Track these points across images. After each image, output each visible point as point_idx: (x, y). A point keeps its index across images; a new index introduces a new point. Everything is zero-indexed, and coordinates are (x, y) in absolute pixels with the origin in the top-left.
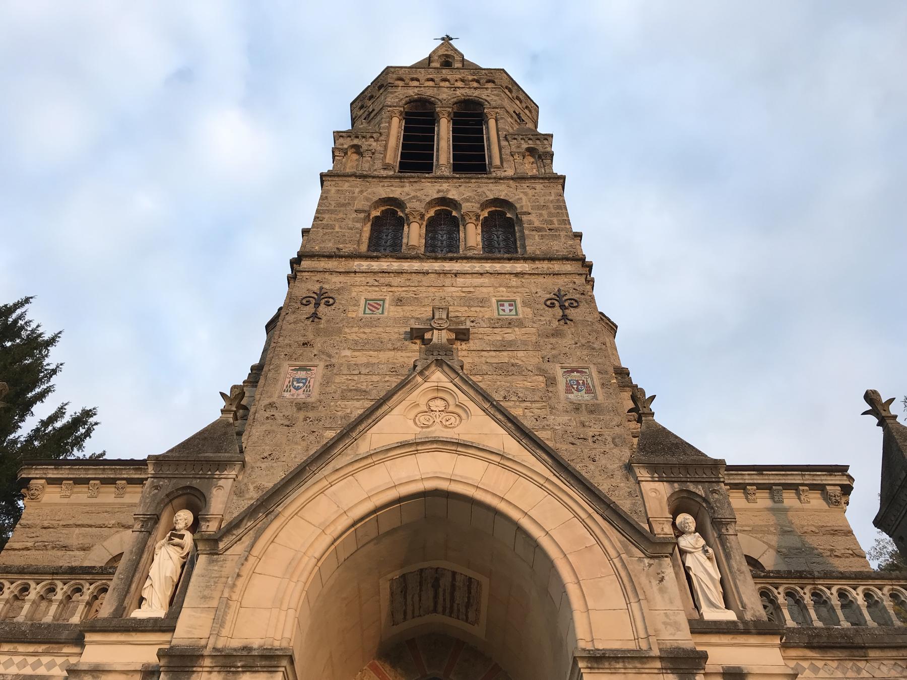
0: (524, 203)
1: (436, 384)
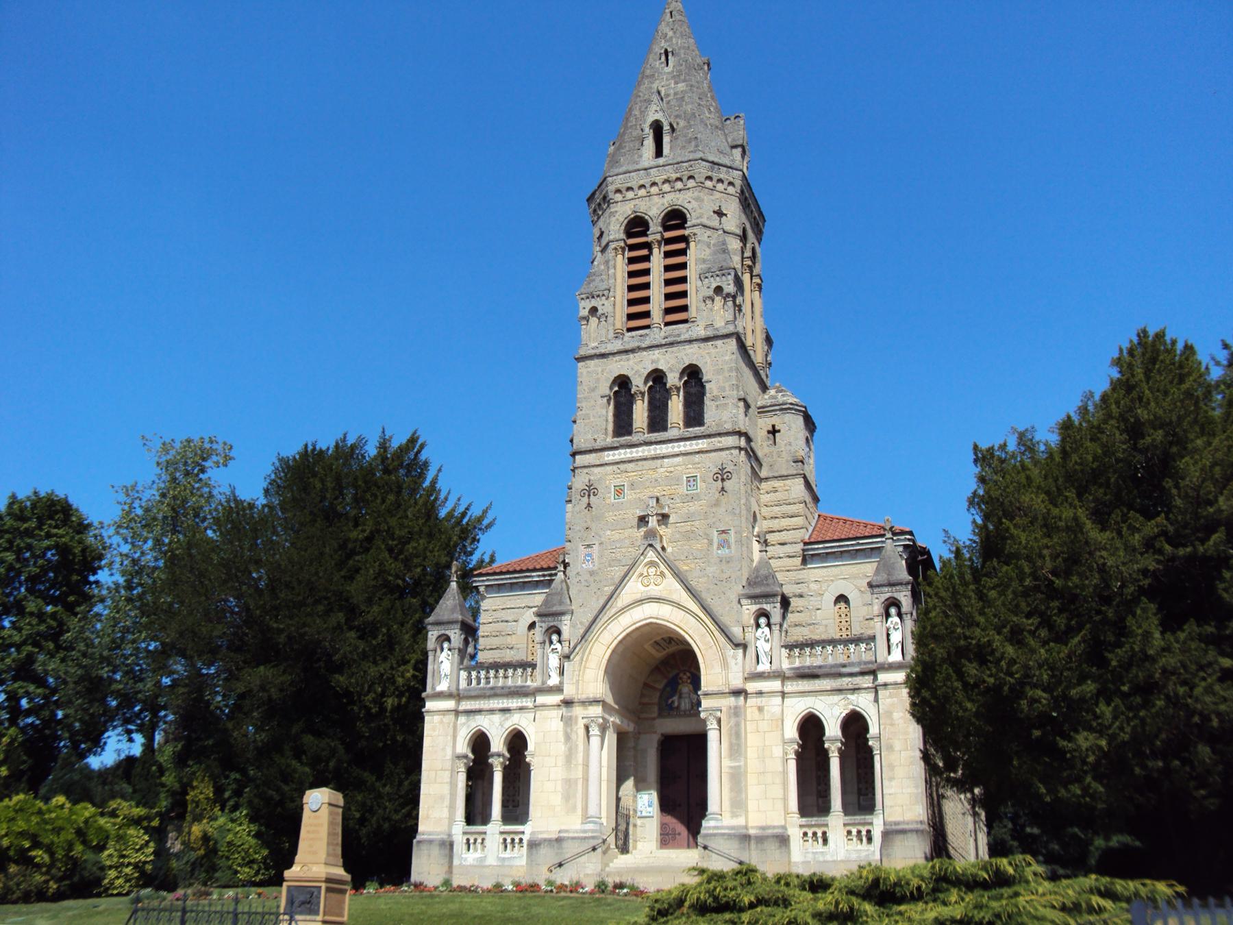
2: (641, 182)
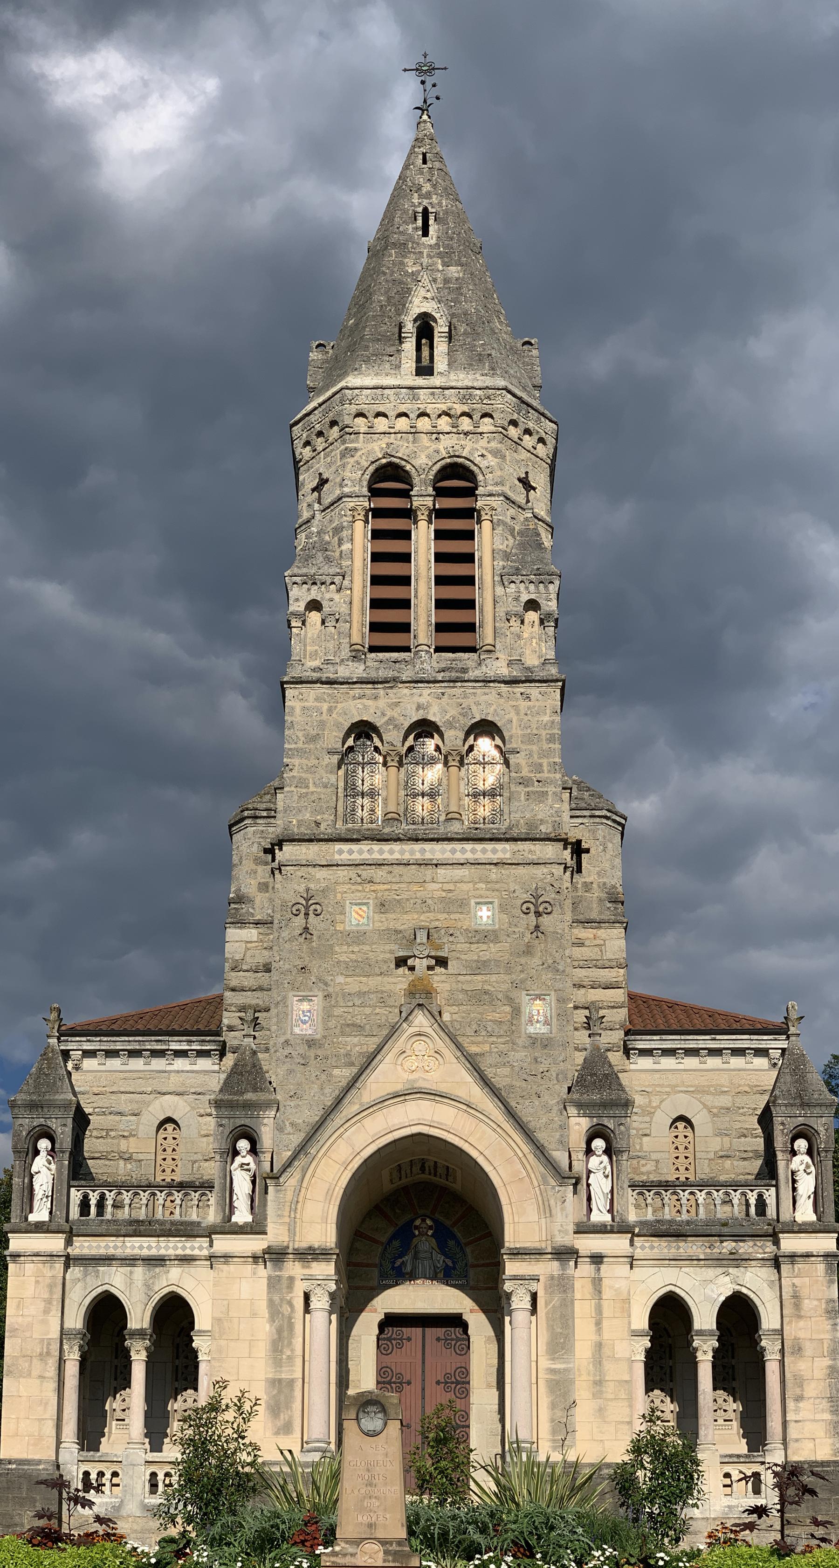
0: (514, 731)
1: (417, 1029)
2: (403, 408)
